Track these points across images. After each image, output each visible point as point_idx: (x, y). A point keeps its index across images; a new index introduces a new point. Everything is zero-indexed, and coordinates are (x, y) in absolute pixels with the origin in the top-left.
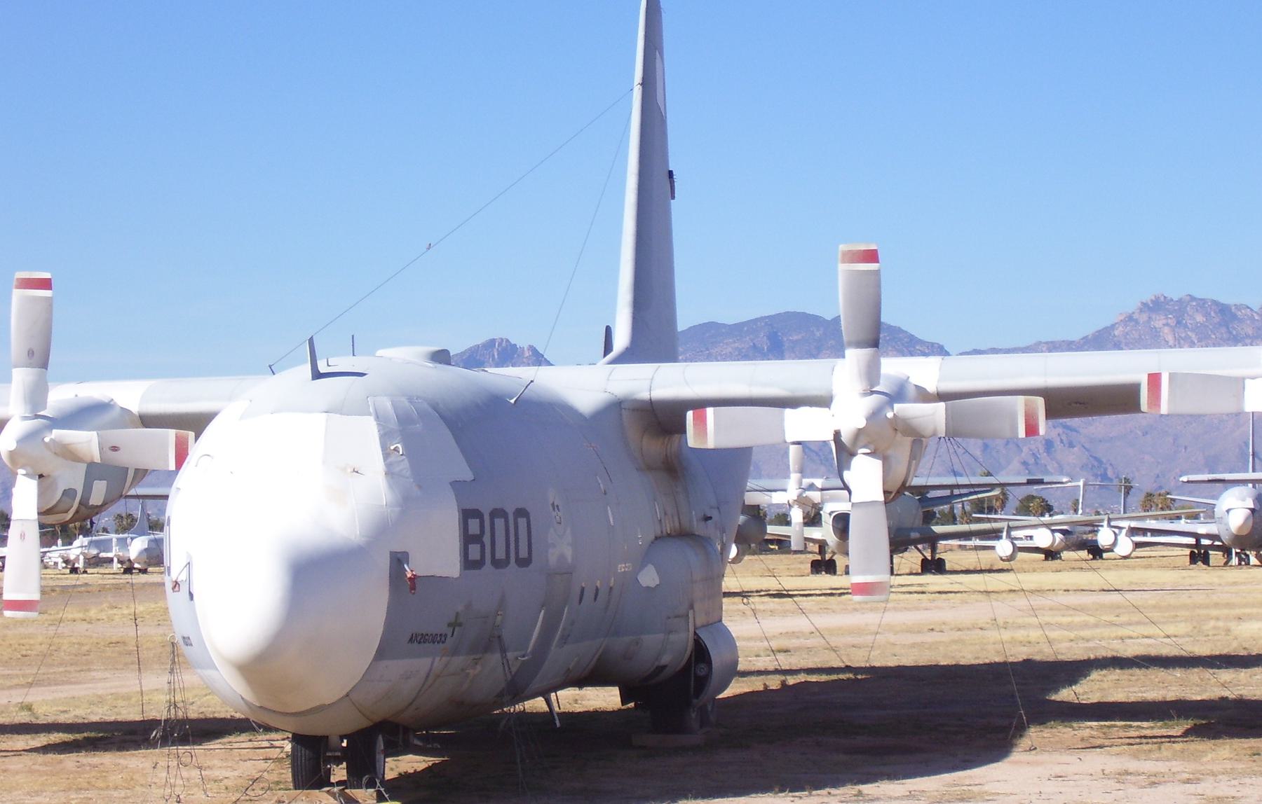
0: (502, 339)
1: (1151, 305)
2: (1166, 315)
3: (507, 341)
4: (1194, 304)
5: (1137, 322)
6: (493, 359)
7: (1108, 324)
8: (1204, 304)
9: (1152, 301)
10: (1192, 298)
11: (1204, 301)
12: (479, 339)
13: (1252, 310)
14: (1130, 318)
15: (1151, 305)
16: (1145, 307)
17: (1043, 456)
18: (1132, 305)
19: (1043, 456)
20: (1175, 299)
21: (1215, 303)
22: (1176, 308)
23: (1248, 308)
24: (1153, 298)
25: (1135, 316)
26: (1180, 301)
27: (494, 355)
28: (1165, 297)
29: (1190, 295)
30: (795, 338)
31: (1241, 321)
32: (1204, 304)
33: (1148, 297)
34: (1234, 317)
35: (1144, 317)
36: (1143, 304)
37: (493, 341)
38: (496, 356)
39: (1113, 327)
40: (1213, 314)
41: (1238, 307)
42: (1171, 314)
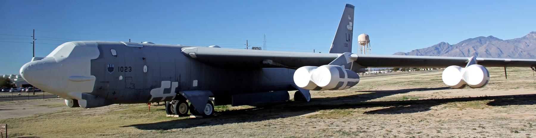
5: (530, 35)
7: (525, 35)
12: (440, 42)
14: (529, 35)
16: (531, 33)
17: (521, 53)
18: (529, 33)
19: (521, 53)
25: (530, 34)
30: (483, 39)
33: (531, 32)
35: (531, 34)
37: (442, 42)
39: (526, 36)
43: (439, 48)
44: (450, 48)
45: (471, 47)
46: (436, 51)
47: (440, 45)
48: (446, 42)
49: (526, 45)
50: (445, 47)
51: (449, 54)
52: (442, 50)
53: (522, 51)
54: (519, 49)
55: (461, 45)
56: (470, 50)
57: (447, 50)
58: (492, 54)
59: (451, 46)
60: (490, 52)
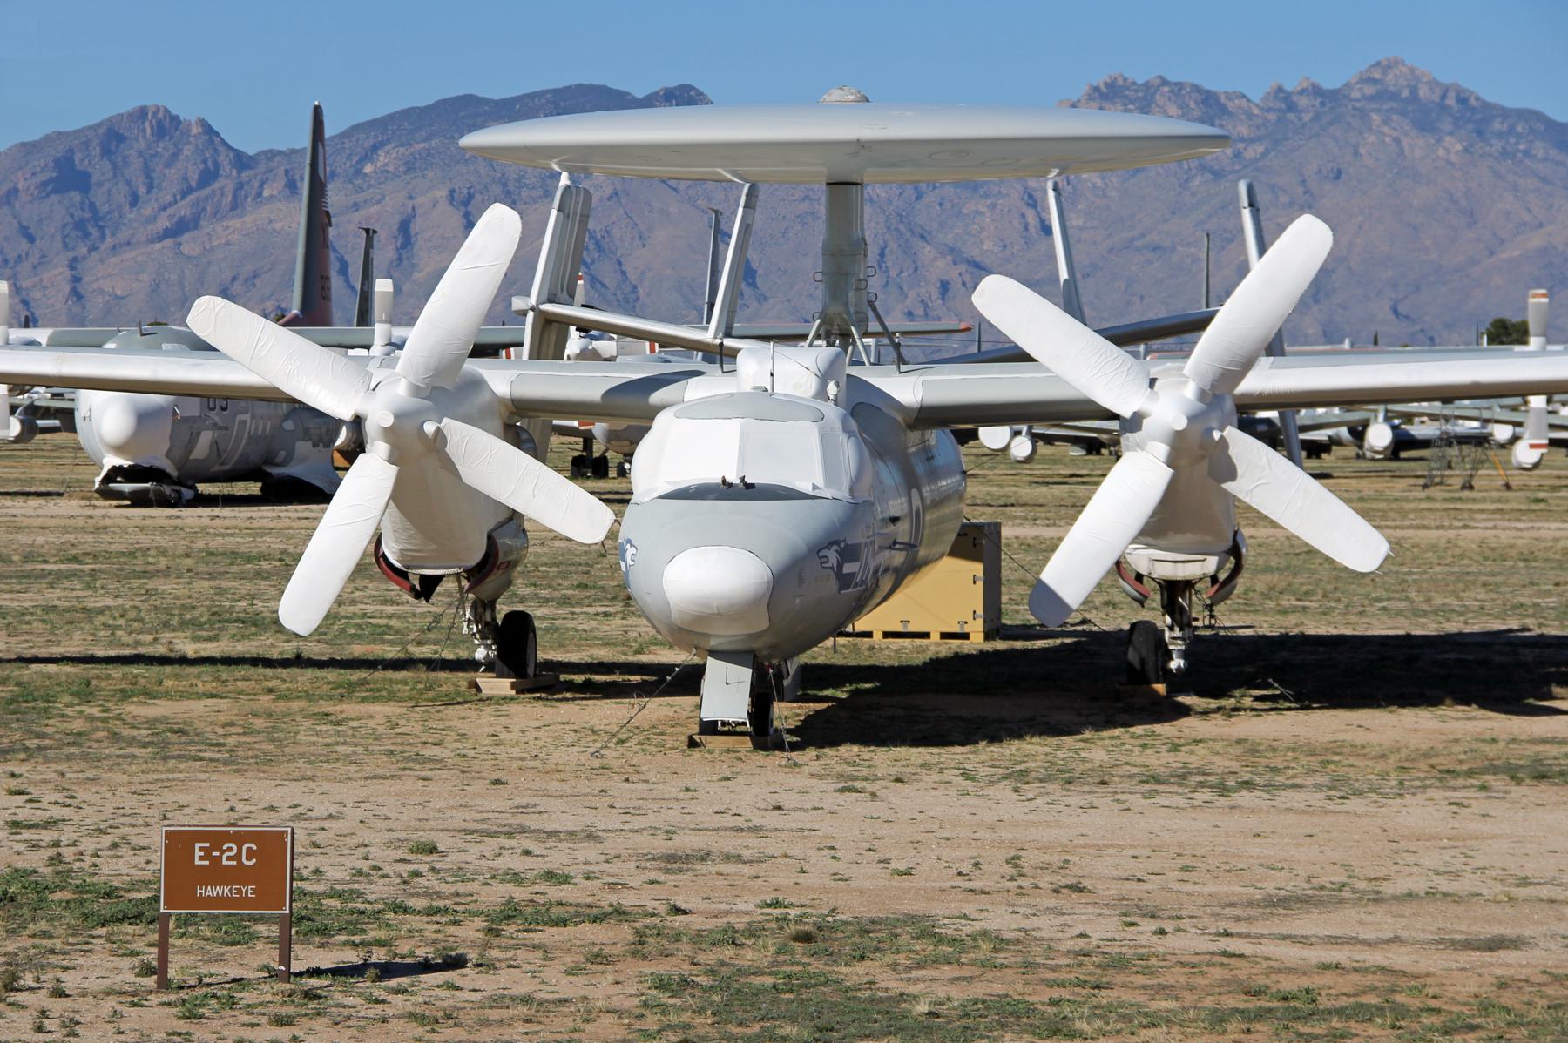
0: (158, 109)
1: (1105, 90)
2: (1125, 105)
3: (166, 110)
4: (1166, 89)
6: (145, 137)
8: (1180, 90)
9: (1106, 84)
10: (1165, 82)
11: (1180, 86)
13: (1249, 100)
15: (1105, 90)
20: (1140, 81)
21: (1197, 89)
22: (1140, 94)
23: (1244, 96)
24: (1108, 80)
26: (1147, 85)
27: (144, 130)
28: (1125, 80)
29: (1161, 77)
31: (1230, 114)
32: (1180, 90)
33: (1100, 79)
34: (1223, 110)
36: (1096, 89)
37: (142, 112)
38: (149, 131)
40: (1192, 105)
41: (1229, 96)
42: (1132, 102)
43: (100, 169)
44: (225, 184)
45: (441, 193)
46: (54, 198)
47: (111, 137)
48: (187, 112)
49: (1023, 216)
50: (173, 173)
51: (185, 249)
52: (134, 201)
53: (945, 287)
54: (926, 251)
55: (358, 172)
56: (415, 227)
57: (184, 209)
58: (641, 292)
59: (242, 161)
60: (628, 268)
